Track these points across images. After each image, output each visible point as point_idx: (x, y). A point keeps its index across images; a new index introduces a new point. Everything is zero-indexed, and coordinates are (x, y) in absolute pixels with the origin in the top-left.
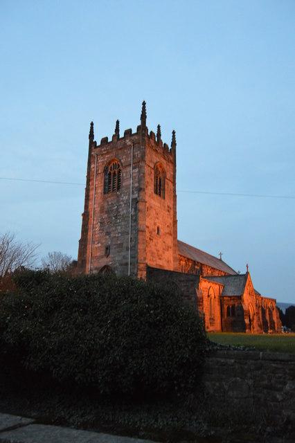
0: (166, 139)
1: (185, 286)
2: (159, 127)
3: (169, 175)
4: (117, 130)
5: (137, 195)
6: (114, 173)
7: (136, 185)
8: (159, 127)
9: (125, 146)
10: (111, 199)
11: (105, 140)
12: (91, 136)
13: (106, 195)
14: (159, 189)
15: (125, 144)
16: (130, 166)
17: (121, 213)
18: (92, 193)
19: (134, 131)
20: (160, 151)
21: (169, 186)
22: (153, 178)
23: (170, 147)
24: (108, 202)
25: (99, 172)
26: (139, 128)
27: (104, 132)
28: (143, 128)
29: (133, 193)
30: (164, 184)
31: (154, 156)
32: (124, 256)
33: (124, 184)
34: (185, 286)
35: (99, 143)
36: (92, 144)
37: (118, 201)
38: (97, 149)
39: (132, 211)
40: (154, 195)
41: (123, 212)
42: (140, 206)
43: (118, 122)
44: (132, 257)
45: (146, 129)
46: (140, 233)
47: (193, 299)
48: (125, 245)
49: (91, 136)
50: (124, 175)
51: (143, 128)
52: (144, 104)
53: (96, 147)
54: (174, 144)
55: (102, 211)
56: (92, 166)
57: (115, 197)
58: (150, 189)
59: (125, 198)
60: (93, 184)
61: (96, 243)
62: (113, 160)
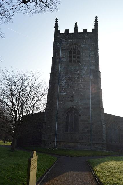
12: (56, 26)
16: (75, 51)
19: (90, 30)
25: (64, 48)
29: (91, 66)
35: (62, 31)
36: (57, 32)
44: (92, 104)
49: (56, 26)
50: (84, 54)
52: (96, 18)
55: (67, 72)
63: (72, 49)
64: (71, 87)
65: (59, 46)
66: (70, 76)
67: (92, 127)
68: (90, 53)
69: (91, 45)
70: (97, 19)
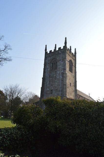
0: (73, 51)
2: (70, 47)
3: (74, 65)
4: (55, 48)
7: (63, 67)
8: (70, 47)
9: (59, 53)
11: (51, 51)
12: (46, 50)
14: (71, 70)
15: (59, 53)
19: (62, 48)
20: (71, 55)
21: (74, 68)
22: (69, 65)
23: (74, 54)
24: (52, 74)
26: (64, 47)
27: (51, 48)
28: (65, 47)
29: (62, 70)
30: (73, 66)
31: (69, 57)
32: (58, 94)
33: (58, 67)
35: (48, 52)
36: (46, 53)
37: (56, 73)
39: (61, 77)
40: (69, 72)
42: (65, 75)
43: (56, 45)
44: (61, 94)
45: (66, 47)
46: (65, 85)
48: (58, 90)
49: (46, 50)
50: (58, 64)
51: (65, 47)
52: (66, 38)
54: (75, 53)
55: (50, 77)
58: (68, 69)
60: (46, 67)
61: (47, 88)
64: (52, 85)
66: (51, 79)
69: (62, 57)
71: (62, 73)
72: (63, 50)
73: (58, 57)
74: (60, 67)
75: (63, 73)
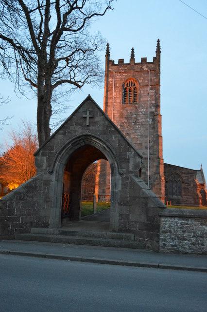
1: (186, 177)
4: (133, 55)
5: (154, 110)
6: (130, 90)
7: (154, 102)
9: (142, 70)
10: (129, 109)
13: (125, 105)
15: (142, 69)
17: (140, 121)
18: (110, 101)
19: (150, 60)
24: (127, 111)
26: (155, 59)
29: (150, 107)
33: (142, 99)
34: (186, 177)
35: (116, 62)
37: (137, 112)
38: (115, 67)
39: (150, 121)
41: (142, 119)
44: (150, 154)
47: (192, 185)
48: (143, 145)
50: (142, 92)
52: (158, 41)
53: (113, 65)
56: (110, 80)
57: (134, 108)
59: (144, 110)
60: (111, 94)
62: (130, 79)
63: (127, 86)
65: (111, 83)
66: (125, 121)
67: (150, 179)
68: (149, 91)
69: (151, 80)
70: (160, 43)
71: (152, 113)
72: (153, 66)
73: (141, 78)
74: (145, 99)
75: (153, 112)
